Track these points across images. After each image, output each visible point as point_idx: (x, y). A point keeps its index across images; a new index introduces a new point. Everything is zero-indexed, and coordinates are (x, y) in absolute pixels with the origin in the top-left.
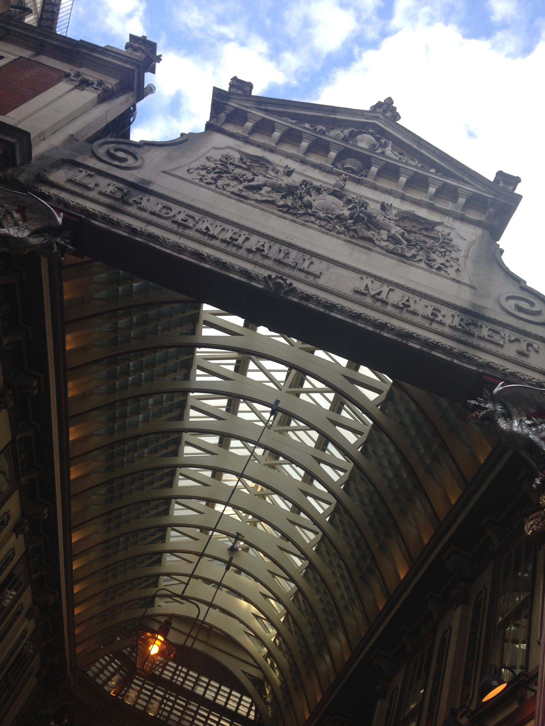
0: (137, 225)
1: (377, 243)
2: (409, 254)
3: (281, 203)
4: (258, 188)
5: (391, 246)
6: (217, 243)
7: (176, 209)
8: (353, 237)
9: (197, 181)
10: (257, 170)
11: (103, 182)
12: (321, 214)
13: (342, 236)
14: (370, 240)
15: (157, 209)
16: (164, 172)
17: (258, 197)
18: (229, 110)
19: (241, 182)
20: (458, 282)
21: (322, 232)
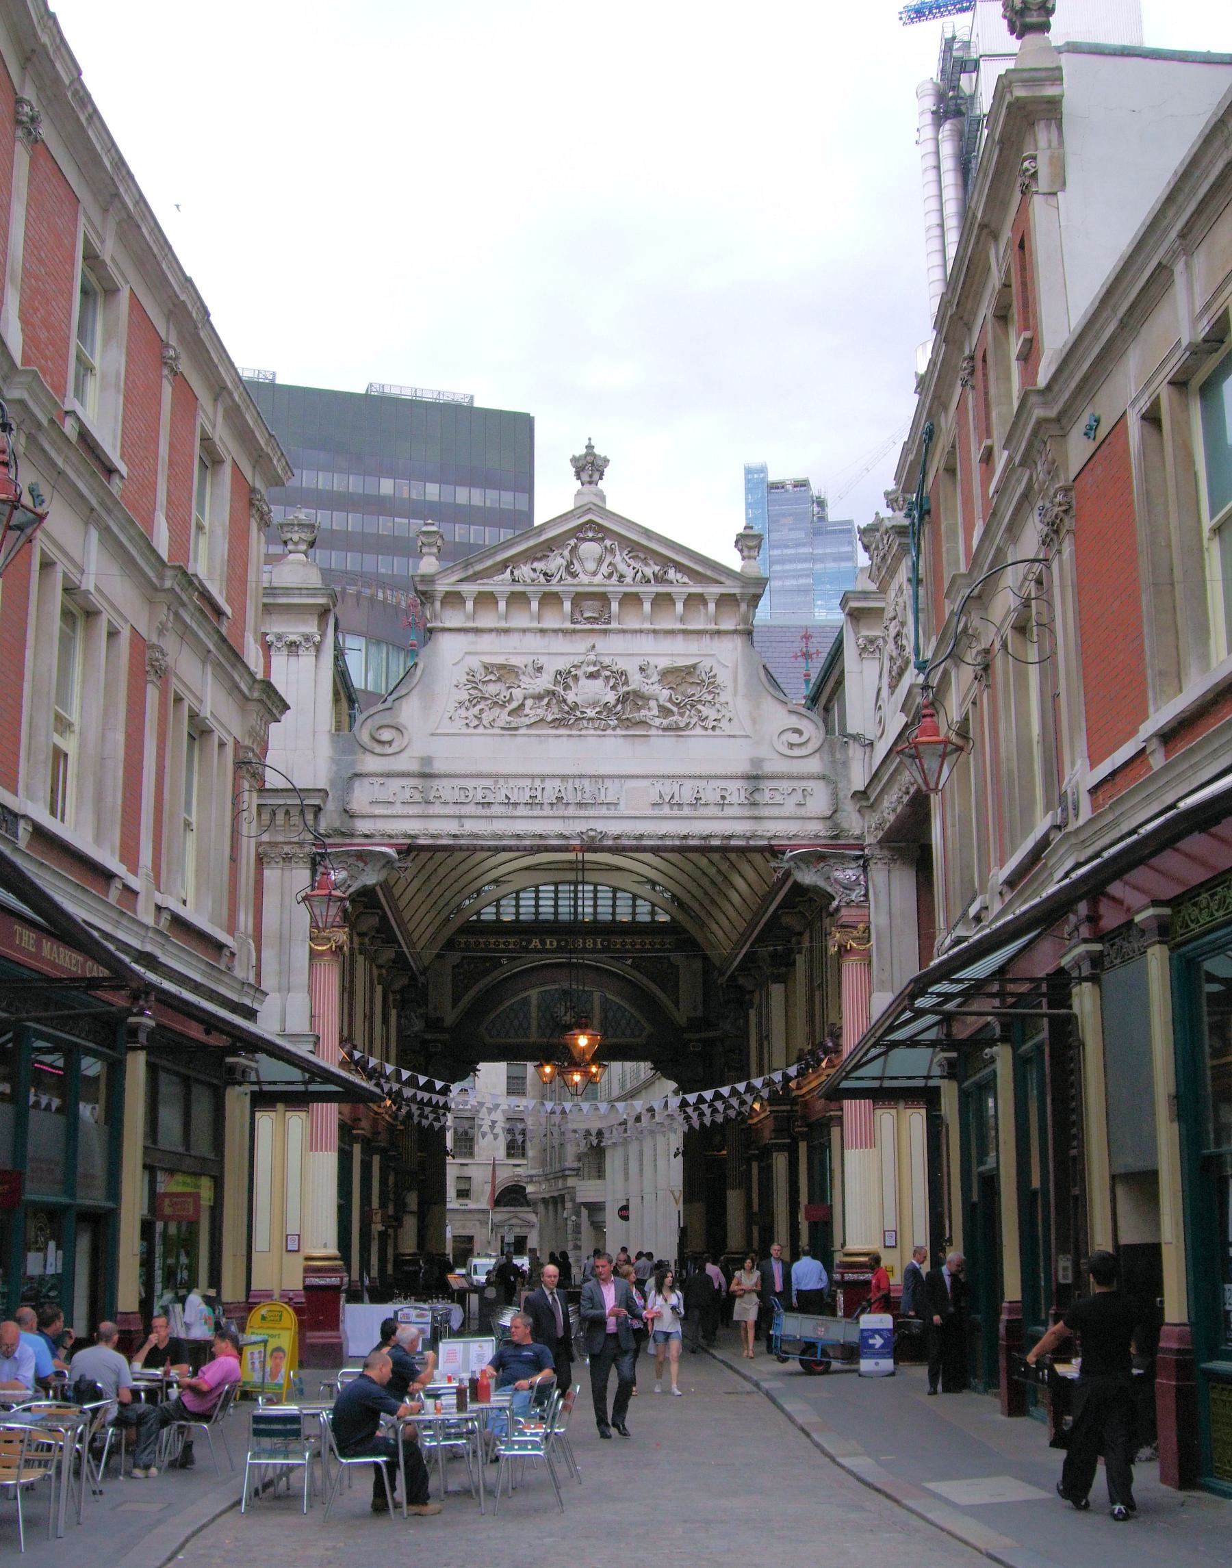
0: (452, 827)
1: (651, 723)
2: (682, 725)
3: (550, 718)
4: (522, 705)
5: (666, 722)
6: (521, 811)
7: (469, 783)
8: (627, 728)
9: (465, 730)
10: (511, 680)
11: (394, 784)
12: (591, 713)
13: (619, 732)
14: (643, 723)
15: (457, 795)
16: (432, 734)
17: (527, 721)
18: (439, 596)
19: (503, 706)
20: (734, 736)
21: (599, 736)
